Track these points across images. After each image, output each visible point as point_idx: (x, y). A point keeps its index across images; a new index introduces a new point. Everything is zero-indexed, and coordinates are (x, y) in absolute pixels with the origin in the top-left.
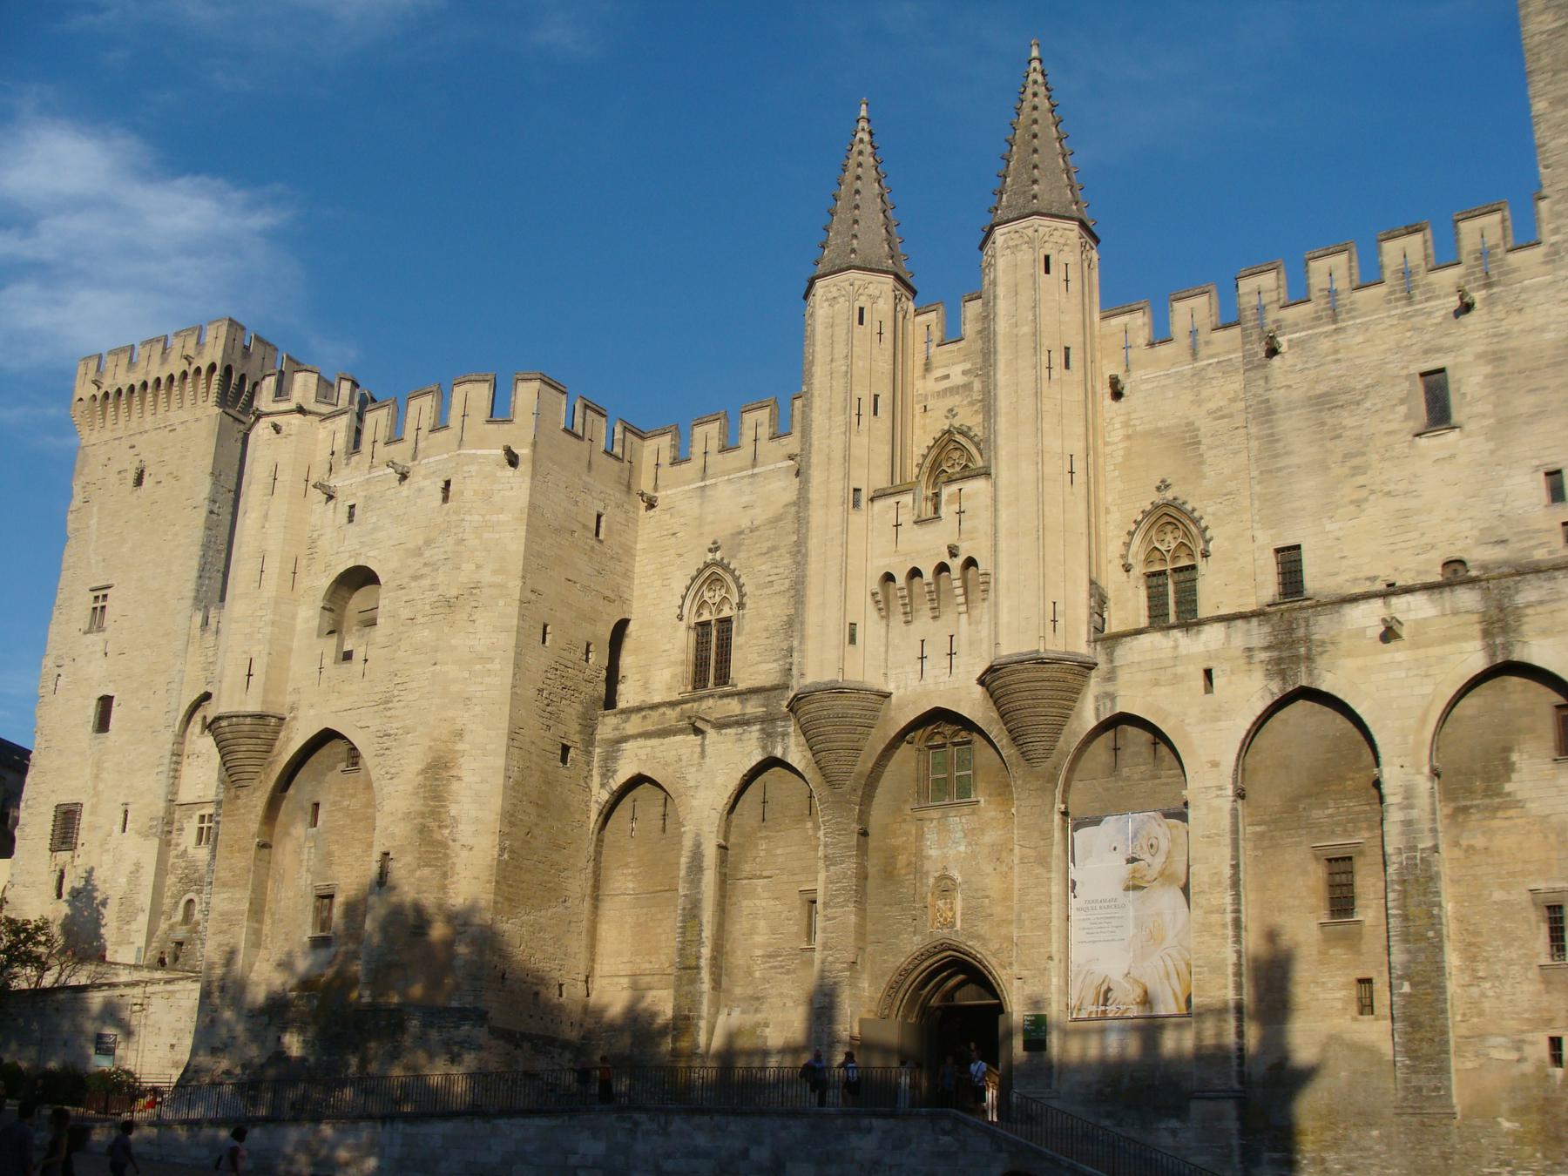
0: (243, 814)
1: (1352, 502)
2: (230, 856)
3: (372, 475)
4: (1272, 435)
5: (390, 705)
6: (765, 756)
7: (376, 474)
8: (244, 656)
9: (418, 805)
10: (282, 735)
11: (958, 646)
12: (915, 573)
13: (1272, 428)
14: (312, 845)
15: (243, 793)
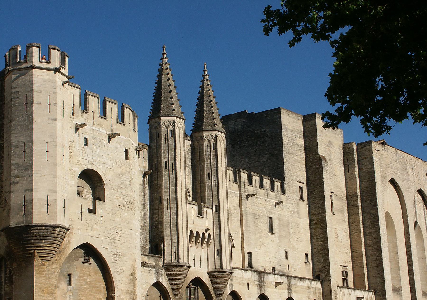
0: (48, 274)
1: (260, 245)
2: (42, 295)
3: (94, 128)
4: (247, 220)
5: (115, 241)
6: (157, 281)
7: (97, 129)
8: (62, 197)
9: (131, 289)
10: (65, 239)
11: (202, 259)
12: (197, 233)
13: (247, 218)
14: (71, 294)
15: (46, 263)
